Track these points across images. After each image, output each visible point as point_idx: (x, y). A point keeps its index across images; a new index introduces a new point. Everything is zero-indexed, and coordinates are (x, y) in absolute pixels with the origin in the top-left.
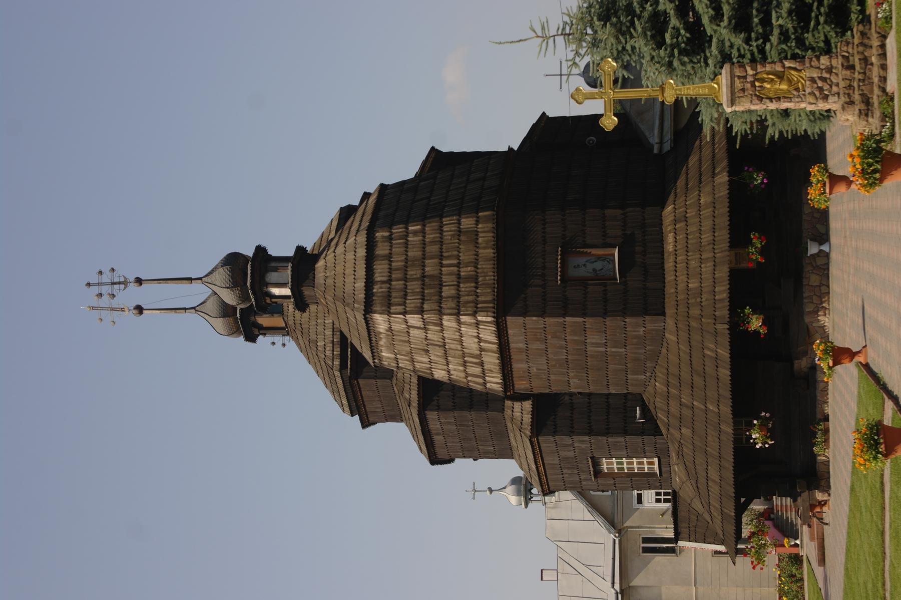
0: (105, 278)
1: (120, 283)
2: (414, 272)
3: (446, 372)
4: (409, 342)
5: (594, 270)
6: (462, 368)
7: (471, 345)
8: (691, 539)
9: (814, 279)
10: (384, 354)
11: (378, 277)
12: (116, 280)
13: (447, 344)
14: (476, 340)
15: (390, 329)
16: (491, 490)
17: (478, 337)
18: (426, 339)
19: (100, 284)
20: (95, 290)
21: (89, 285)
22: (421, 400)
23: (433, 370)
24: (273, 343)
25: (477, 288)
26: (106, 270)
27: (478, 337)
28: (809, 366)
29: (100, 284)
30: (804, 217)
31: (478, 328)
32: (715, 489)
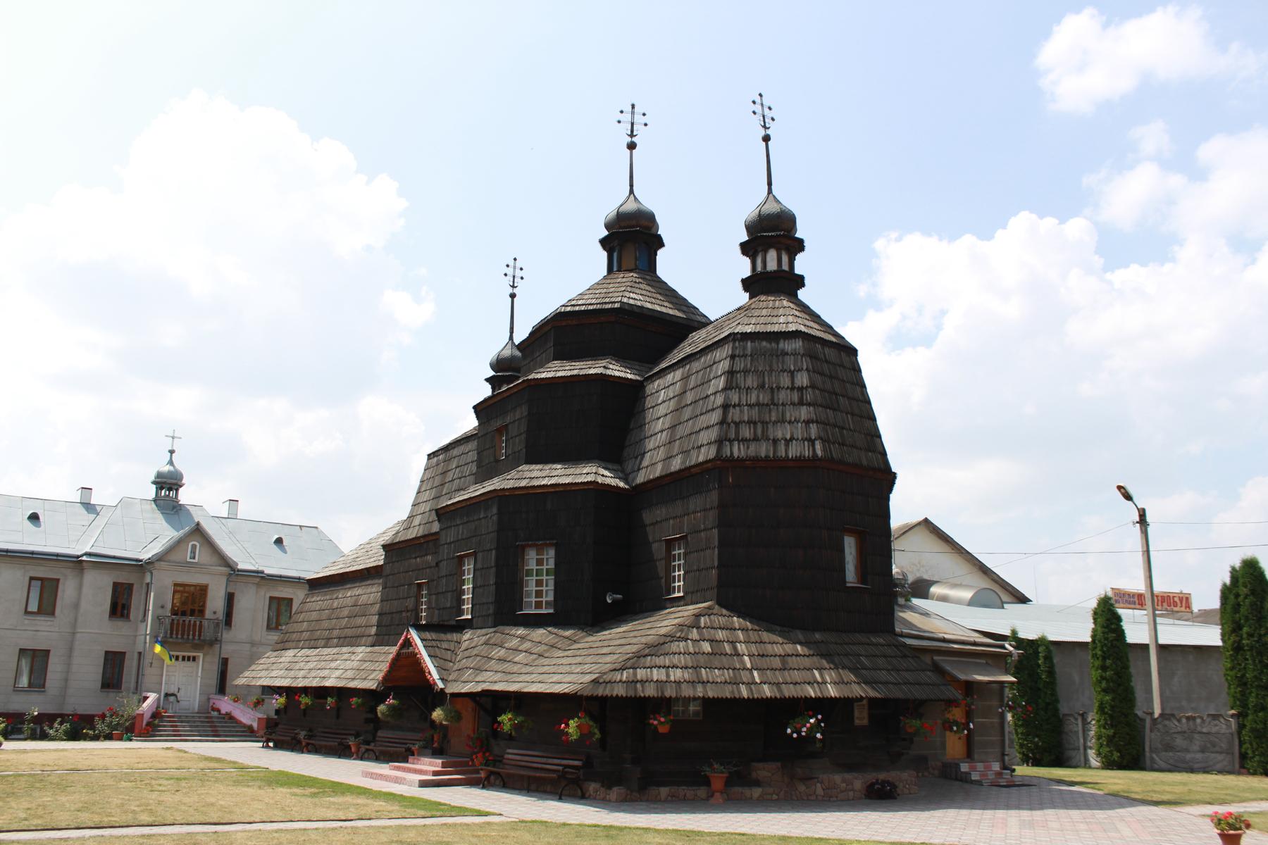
3: (737, 403)
4: (771, 370)
6: (746, 419)
7: (782, 432)
8: (424, 642)
10: (749, 344)
11: (827, 350)
12: (766, 120)
13: (775, 407)
14: (788, 437)
16: (172, 452)
17: (792, 439)
18: (779, 388)
20: (758, 100)
21: (761, 95)
22: (611, 380)
23: (737, 390)
24: (508, 266)
25: (839, 444)
27: (792, 439)
30: (898, 773)
31: (803, 440)
32: (657, 674)
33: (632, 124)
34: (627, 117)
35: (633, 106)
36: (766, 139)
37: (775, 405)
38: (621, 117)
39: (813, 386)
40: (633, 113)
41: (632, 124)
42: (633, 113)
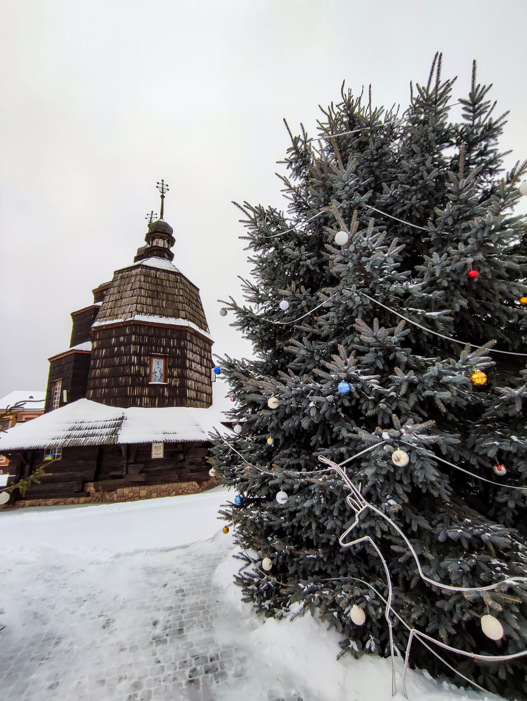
0: (165, 187)
1: (163, 190)
2: (160, 289)
5: (155, 372)
9: (143, 493)
15: (132, 276)
19: (163, 184)
20: (161, 182)
21: (163, 180)
26: (168, 188)
28: (91, 492)
29: (163, 184)
30: (180, 484)
33: (151, 218)
34: (150, 216)
35: (152, 212)
36: (163, 197)
37: (121, 299)
38: (147, 217)
39: (140, 288)
40: (152, 214)
41: (151, 218)
42: (152, 214)
